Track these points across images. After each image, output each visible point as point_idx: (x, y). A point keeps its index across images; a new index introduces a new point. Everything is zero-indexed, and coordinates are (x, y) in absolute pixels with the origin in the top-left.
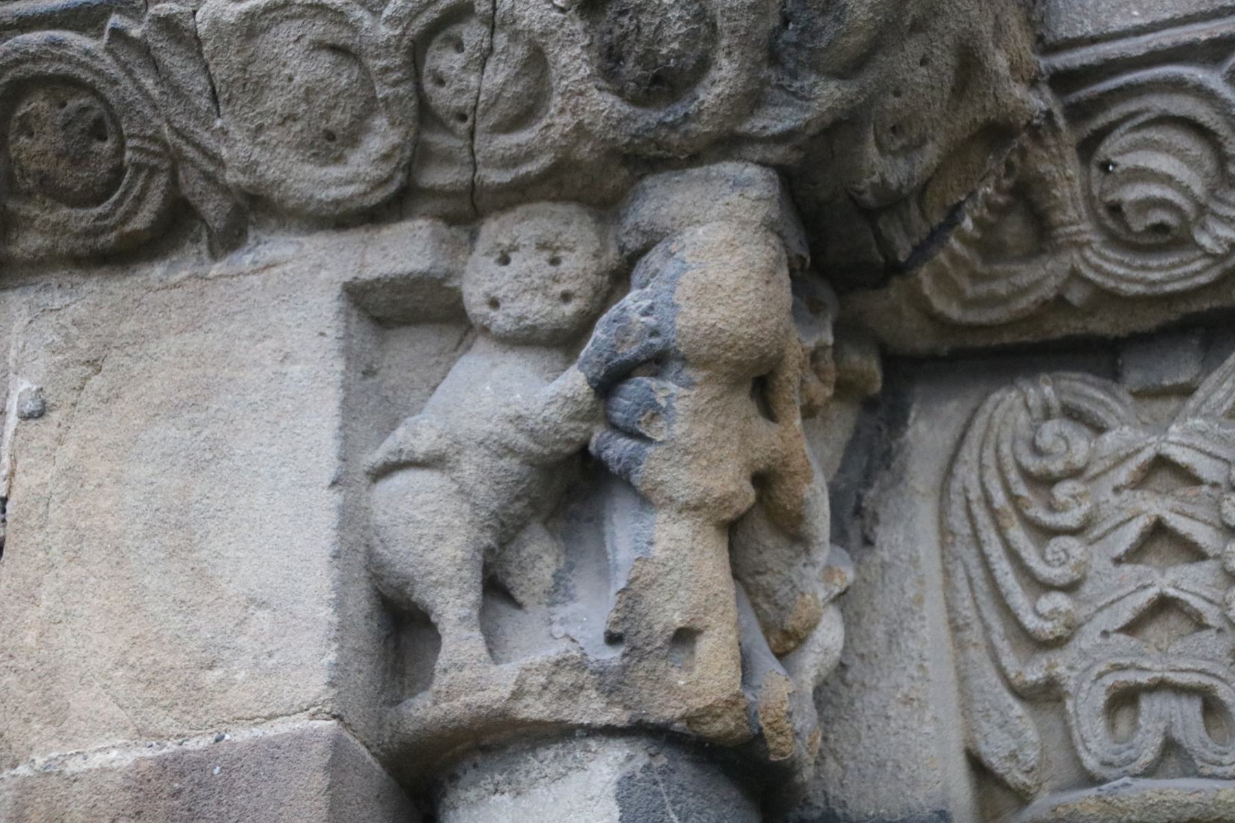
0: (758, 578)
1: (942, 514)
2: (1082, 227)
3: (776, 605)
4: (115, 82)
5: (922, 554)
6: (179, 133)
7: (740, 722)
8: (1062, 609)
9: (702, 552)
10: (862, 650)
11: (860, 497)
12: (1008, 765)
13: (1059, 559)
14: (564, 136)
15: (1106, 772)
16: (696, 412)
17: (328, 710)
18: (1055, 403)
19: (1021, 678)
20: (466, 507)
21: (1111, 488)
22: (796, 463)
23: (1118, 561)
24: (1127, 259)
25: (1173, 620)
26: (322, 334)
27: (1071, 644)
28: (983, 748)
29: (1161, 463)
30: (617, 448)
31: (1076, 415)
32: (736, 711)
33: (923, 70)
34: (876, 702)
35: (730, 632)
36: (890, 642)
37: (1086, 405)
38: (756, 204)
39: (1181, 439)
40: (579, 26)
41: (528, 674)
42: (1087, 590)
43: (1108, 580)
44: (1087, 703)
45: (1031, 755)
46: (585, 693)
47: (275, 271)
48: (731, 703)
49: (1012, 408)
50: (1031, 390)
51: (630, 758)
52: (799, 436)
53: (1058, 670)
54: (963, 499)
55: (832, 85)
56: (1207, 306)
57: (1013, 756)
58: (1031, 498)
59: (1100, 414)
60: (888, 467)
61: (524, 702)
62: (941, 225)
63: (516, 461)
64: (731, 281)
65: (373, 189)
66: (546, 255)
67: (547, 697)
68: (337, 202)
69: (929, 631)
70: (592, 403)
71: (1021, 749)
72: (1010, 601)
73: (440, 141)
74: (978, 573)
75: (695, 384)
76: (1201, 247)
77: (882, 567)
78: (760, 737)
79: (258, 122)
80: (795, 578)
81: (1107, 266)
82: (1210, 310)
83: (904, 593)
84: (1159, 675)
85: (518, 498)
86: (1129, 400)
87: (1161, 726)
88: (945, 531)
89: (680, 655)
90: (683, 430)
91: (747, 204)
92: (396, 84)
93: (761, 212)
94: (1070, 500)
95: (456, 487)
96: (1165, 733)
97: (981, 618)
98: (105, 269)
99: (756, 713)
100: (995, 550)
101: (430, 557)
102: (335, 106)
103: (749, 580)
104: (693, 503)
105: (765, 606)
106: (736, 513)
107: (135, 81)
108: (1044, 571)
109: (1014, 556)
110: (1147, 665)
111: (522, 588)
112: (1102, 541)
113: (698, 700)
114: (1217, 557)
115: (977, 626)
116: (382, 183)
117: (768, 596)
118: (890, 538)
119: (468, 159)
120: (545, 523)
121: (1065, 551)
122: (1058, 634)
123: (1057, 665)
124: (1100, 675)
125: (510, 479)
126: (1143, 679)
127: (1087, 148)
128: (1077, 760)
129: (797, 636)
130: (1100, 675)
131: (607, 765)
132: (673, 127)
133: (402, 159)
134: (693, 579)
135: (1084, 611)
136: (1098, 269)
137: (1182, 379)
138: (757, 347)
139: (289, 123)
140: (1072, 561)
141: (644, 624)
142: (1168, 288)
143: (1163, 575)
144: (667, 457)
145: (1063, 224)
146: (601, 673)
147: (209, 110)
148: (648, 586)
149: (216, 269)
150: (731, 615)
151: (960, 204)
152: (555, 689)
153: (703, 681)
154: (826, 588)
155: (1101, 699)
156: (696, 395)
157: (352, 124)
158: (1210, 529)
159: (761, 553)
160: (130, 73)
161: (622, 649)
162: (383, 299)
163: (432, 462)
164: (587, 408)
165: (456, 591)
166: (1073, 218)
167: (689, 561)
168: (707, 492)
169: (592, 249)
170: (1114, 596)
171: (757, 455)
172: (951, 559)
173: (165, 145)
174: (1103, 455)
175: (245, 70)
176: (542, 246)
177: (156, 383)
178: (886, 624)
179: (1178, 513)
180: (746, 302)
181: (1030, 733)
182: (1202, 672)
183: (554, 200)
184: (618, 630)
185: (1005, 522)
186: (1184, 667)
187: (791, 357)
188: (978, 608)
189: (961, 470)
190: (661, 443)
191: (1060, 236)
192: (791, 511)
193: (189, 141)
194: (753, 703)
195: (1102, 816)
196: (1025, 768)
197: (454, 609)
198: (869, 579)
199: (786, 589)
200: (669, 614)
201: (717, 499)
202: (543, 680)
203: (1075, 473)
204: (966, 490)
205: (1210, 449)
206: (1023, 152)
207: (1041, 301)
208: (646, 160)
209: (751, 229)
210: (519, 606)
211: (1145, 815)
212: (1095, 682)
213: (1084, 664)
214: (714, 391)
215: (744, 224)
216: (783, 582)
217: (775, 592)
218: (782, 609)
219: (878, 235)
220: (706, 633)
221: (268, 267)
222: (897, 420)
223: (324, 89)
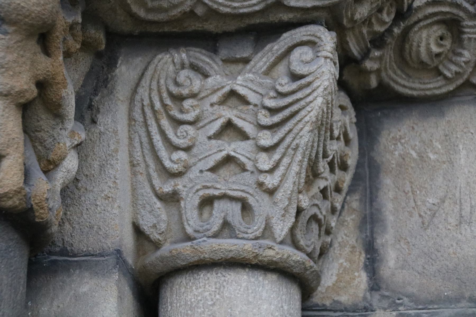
0: (37, 133)
1: (130, 110)
3: (45, 147)
5: (119, 129)
7: (21, 201)
8: (183, 159)
9: (8, 117)
10: (87, 173)
11: (91, 100)
12: (152, 230)
13: (183, 136)
15: (196, 235)
16: (8, 47)
18: (186, 62)
19: (161, 190)
21: (209, 104)
22: (59, 78)
23: (210, 138)
25: (232, 167)
27: (186, 175)
28: (141, 222)
29: (233, 93)
32: (20, 196)
35: (20, 158)
36: (101, 170)
37: (201, 64)
39: (242, 83)
42: (195, 150)
43: (204, 147)
44: (190, 203)
45: (163, 226)
48: (18, 192)
49: (168, 64)
50: (176, 55)
52: (61, 65)
53: (178, 187)
54: (141, 105)
56: (258, 21)
57: (154, 226)
58: (172, 106)
59: (207, 69)
60: (106, 87)
69: (120, 165)
71: (158, 223)
72: (159, 154)
74: (145, 140)
77: (100, 134)
78: (31, 209)
80: (55, 135)
82: (260, 24)
83: (109, 147)
84: (224, 191)
86: (220, 63)
87: (223, 215)
88: (131, 119)
94: (190, 108)
96: (224, 218)
97: (145, 161)
99: (30, 198)
100: (154, 130)
103: (32, 134)
104: (5, 93)
105: (40, 148)
106: (27, 99)
109: (162, 133)
110: (218, 186)
112: (204, 128)
114: (254, 139)
115: (143, 165)
117: (41, 143)
118: (104, 121)
121: (186, 131)
122: (180, 170)
123: (178, 185)
124: (197, 191)
126: (217, 193)
128: (184, 229)
129: (55, 163)
130: (197, 191)
134: (2, 130)
135: (192, 161)
137: (245, 55)
138: (41, 18)
140: (189, 137)
142: (241, 11)
143: (229, 145)
154: (71, 141)
155: (197, 201)
156: (9, 39)
158: (252, 126)
159: (39, 121)
168: (12, 88)
170: (207, 154)
171: (39, 72)
172: (133, 132)
174: (207, 88)
178: (99, 161)
179: (238, 117)
181: (163, 216)
182: (243, 191)
185: (159, 117)
186: (235, 188)
187: (59, 26)
188: (144, 156)
189: (140, 90)
192: (55, 102)
194: (29, 193)
195: (192, 255)
196: (159, 232)
198: (93, 139)
201: (17, 92)
203: (193, 96)
204: (142, 100)
205: (255, 88)
207: (183, 12)
211: (211, 255)
212: (195, 193)
214: (18, 38)
216: (49, 136)
217: (45, 141)
220: (7, 157)
222: (112, 64)
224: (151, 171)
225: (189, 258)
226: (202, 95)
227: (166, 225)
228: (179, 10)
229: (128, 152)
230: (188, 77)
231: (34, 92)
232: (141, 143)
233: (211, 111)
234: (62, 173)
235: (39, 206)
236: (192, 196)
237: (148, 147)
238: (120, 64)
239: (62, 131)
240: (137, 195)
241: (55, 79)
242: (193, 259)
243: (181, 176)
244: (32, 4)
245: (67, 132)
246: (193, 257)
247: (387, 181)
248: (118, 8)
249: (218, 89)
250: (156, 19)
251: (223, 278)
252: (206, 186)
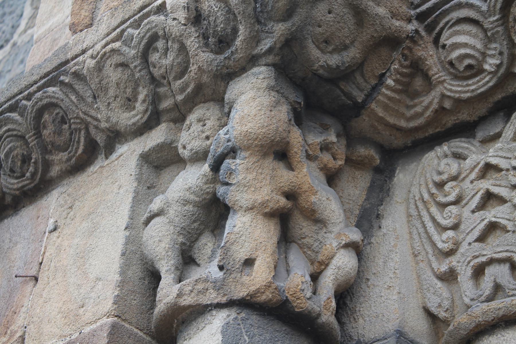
1: (408, 208)
2: (440, 74)
3: (314, 251)
4: (62, 100)
5: (397, 226)
6: (85, 113)
7: (274, 294)
8: (451, 237)
10: (375, 271)
11: (378, 210)
12: (438, 310)
14: (196, 74)
16: (247, 169)
17: (113, 314)
18: (448, 152)
19: (439, 271)
20: (172, 227)
23: (473, 212)
24: (460, 83)
25: (498, 232)
26: (131, 175)
28: (429, 305)
30: (221, 190)
31: (458, 156)
33: (331, 15)
34: (377, 291)
37: (460, 150)
38: (263, 80)
40: (193, 29)
41: (185, 287)
42: (462, 227)
43: (470, 221)
45: (446, 304)
46: (208, 291)
47: (122, 157)
48: (268, 286)
51: (228, 316)
52: (306, 175)
53: (453, 264)
54: (414, 201)
55: (280, 25)
56: (500, 96)
57: (440, 306)
58: (438, 193)
59: (466, 152)
61: (183, 298)
62: (376, 85)
63: (191, 206)
64: (253, 112)
65: (144, 115)
66: (201, 123)
67: (193, 294)
68: (134, 124)
70: (212, 175)
72: (433, 238)
73: (162, 90)
74: (421, 230)
75: (246, 158)
76: (486, 70)
79: (108, 101)
81: (454, 88)
82: (503, 98)
84: (490, 256)
85: (195, 221)
86: (478, 144)
87: (492, 278)
88: (409, 216)
89: (247, 270)
90: (242, 177)
91: (260, 81)
92: (140, 71)
93: (265, 84)
95: (168, 221)
96: (494, 281)
97: (425, 250)
98: (79, 173)
99: (284, 291)
101: (157, 249)
102: (126, 88)
105: (309, 252)
106: (271, 209)
107: (69, 98)
108: (444, 222)
109: (434, 220)
110: (485, 253)
111: (200, 258)
112: (468, 205)
113: (253, 287)
114: (510, 201)
115: (423, 253)
116: (146, 111)
118: (387, 223)
119: (171, 94)
120: (213, 231)
121: (450, 211)
122: (450, 248)
123: (452, 262)
124: (469, 262)
125: (189, 214)
126: (484, 259)
127: (436, 41)
129: (324, 263)
130: (469, 262)
131: (218, 320)
132: (228, 58)
133: (149, 100)
136: (451, 91)
137: (497, 130)
138: (268, 137)
139: (117, 99)
141: (231, 259)
142: (479, 91)
143: (490, 214)
144: (238, 189)
145: (433, 75)
146: (214, 282)
147: (92, 102)
148: (232, 244)
149: (107, 162)
150: (269, 250)
151: (383, 75)
152: (195, 291)
153: (257, 279)
155: (469, 272)
157: (133, 92)
158: (507, 189)
159: (301, 229)
160: (67, 96)
161: (224, 271)
162: (154, 158)
163: (159, 213)
164: (210, 178)
165: (166, 261)
166: (436, 71)
167: (249, 231)
168: (255, 201)
169: (217, 117)
172: (411, 227)
173: (82, 119)
175: (100, 83)
176: (199, 121)
177: (85, 209)
179: (494, 185)
180: (260, 120)
182: (507, 251)
183: (204, 102)
184: (221, 264)
185: (429, 206)
186: (499, 251)
187: (295, 143)
189: (413, 189)
190: (234, 184)
191: (433, 80)
192: (307, 208)
193: (88, 116)
194: (283, 287)
197: (166, 268)
198: (379, 242)
199: (317, 244)
200: (242, 254)
201: (260, 203)
202: (190, 288)
203: (454, 178)
204: (415, 196)
205: (504, 155)
206: (410, 49)
207: (434, 110)
208: (228, 75)
209: (262, 91)
210: (199, 265)
211: (484, 317)
212: (467, 265)
213: (463, 259)
214: (255, 159)
215: (259, 89)
216: (315, 241)
217: (312, 245)
218: (317, 252)
219: (342, 91)
221: (120, 156)
222: (391, 175)
223: (121, 81)
224: (430, 256)
225: (467, 326)
226: (463, 176)
227: (450, 301)
228: (431, 110)
229: (410, 246)
230: (448, 164)
231: (283, 201)
232: (419, 234)
233: (471, 188)
234: (332, 270)
235: (295, 297)
236: (466, 269)
237: (425, 236)
238: (398, 173)
239: (327, 234)
240: (422, 281)
241: (302, 189)
242: (471, 326)
243: (454, 253)
244: (257, 128)
245: (333, 234)
246: (470, 324)
248: (376, 124)
249: (475, 167)
250: (416, 124)
251: (502, 338)
252: (475, 256)
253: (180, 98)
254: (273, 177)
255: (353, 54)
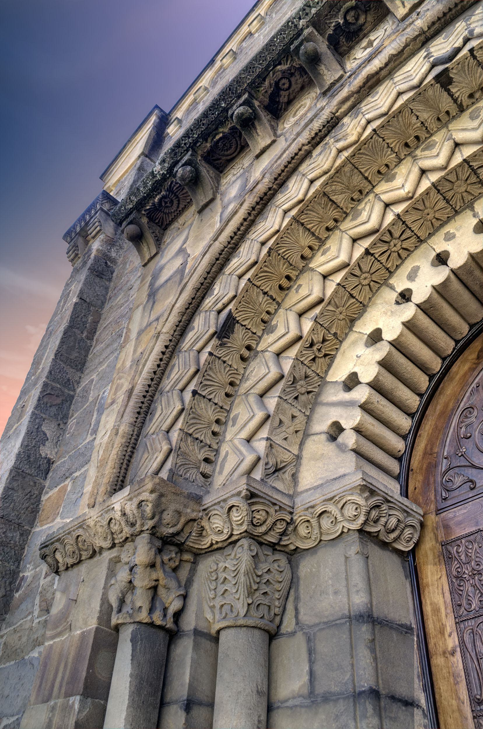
155: (219, 607)
247: (301, 582)
253: (121, 540)
254: (150, 575)
255: (179, 527)
